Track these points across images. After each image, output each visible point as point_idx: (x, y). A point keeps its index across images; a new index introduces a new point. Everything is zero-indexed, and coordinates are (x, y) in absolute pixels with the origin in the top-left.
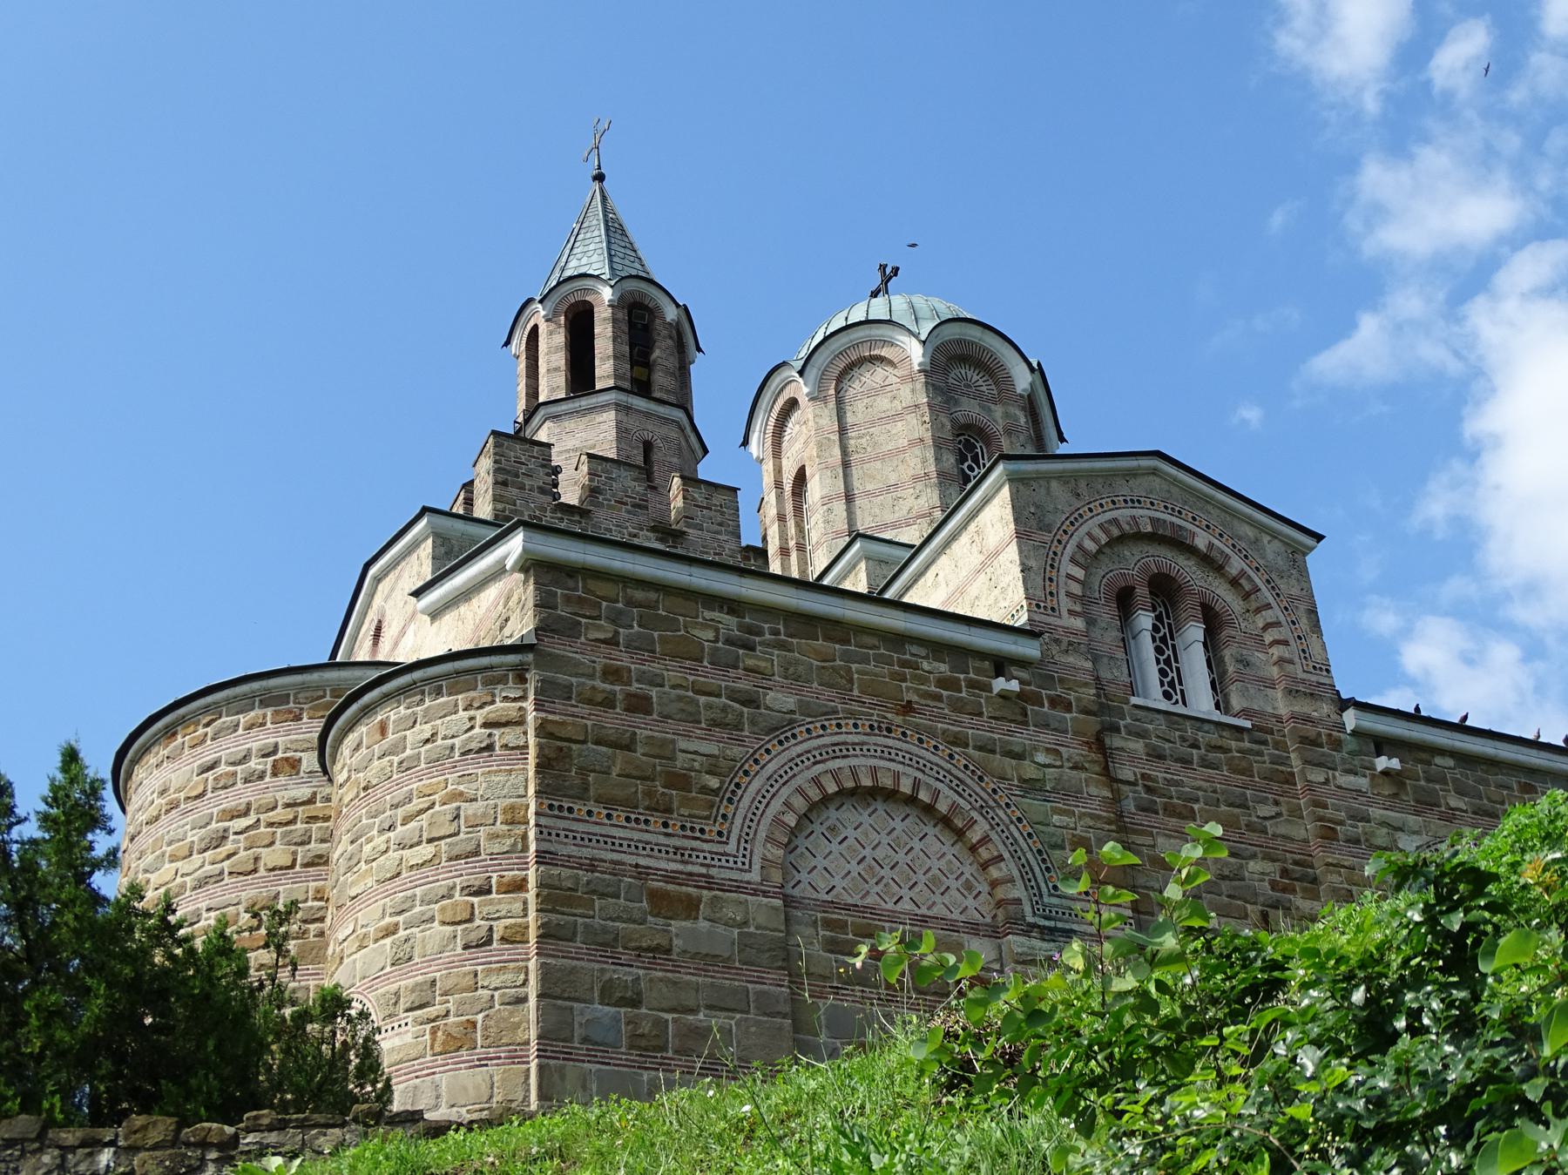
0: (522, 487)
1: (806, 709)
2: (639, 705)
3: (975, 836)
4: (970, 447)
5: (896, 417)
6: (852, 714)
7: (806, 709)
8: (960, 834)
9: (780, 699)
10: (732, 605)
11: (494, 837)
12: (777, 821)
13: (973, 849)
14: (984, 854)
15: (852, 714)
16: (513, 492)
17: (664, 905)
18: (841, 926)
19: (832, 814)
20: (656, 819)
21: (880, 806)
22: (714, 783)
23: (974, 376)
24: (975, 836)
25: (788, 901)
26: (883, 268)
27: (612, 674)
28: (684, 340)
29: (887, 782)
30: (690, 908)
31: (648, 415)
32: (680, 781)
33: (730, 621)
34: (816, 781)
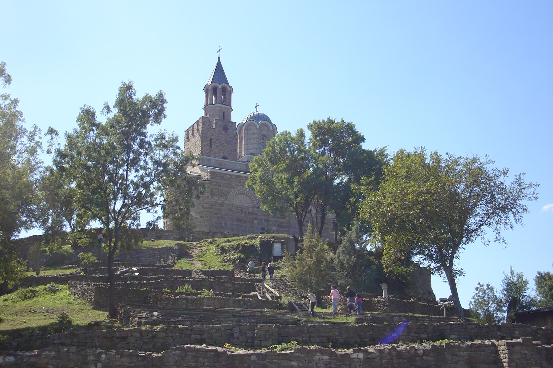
0: (206, 125)
1: (236, 185)
2: (220, 186)
3: (252, 198)
4: (263, 137)
5: (254, 134)
6: (241, 186)
7: (236, 185)
8: (250, 198)
9: (234, 185)
10: (230, 175)
11: (206, 199)
12: (232, 197)
13: (252, 199)
14: (253, 200)
15: (241, 186)
16: (204, 126)
17: (221, 205)
18: (237, 207)
19: (238, 196)
20: (221, 197)
21: (243, 195)
22: (226, 193)
23: (265, 127)
24: (252, 198)
25: (232, 205)
26: (257, 104)
27: (217, 183)
28: (231, 91)
29: (243, 193)
30: (223, 206)
31: (224, 107)
32: (223, 193)
33: (229, 176)
34: (236, 193)
